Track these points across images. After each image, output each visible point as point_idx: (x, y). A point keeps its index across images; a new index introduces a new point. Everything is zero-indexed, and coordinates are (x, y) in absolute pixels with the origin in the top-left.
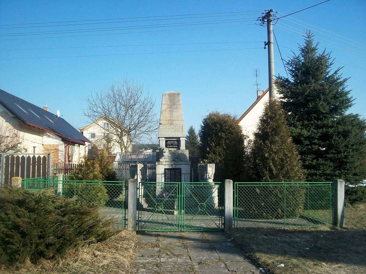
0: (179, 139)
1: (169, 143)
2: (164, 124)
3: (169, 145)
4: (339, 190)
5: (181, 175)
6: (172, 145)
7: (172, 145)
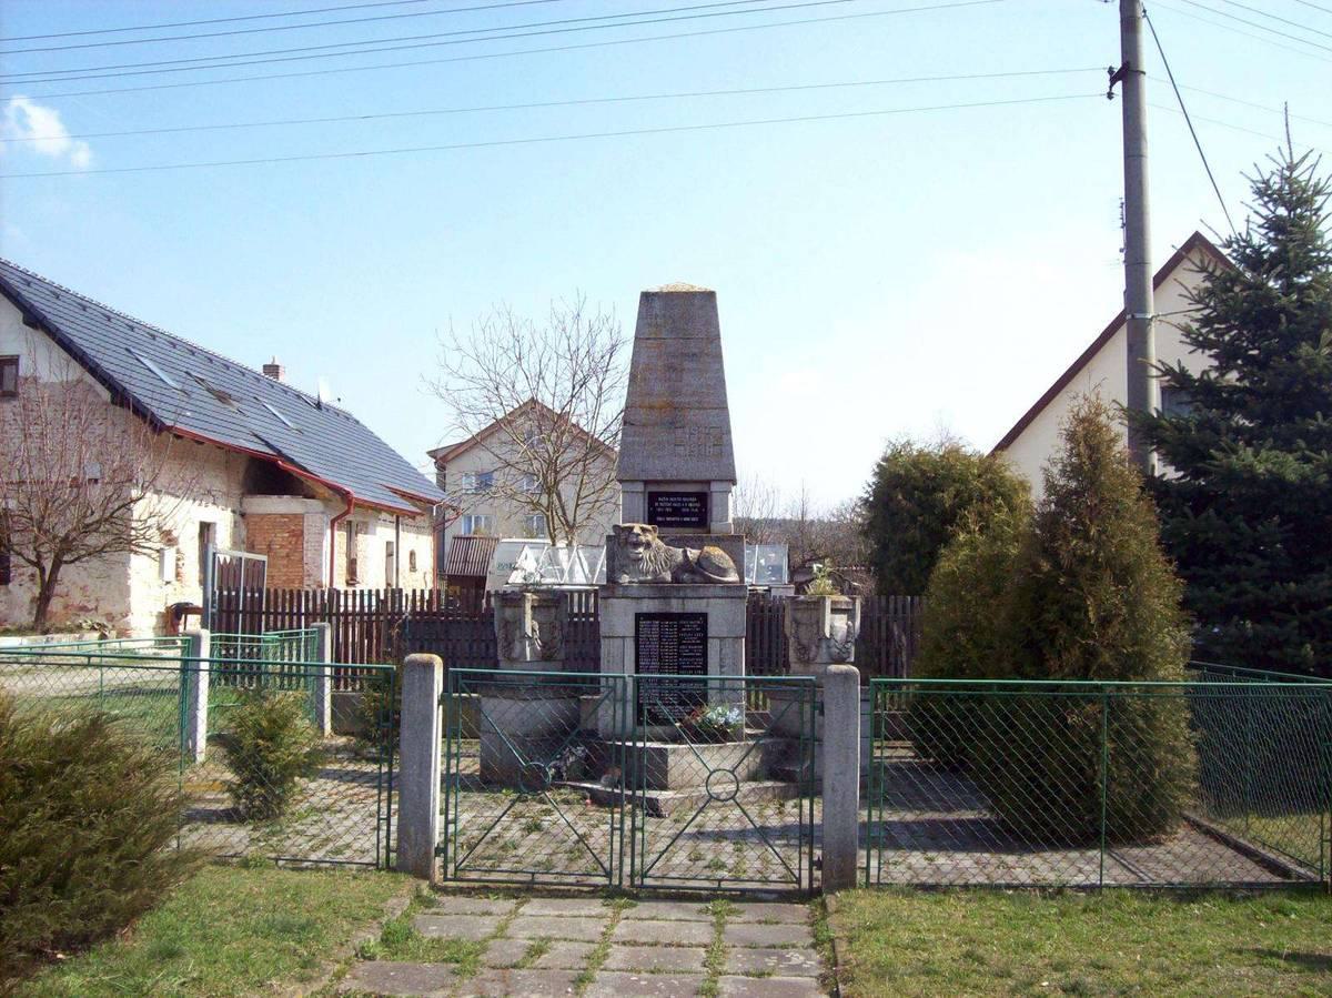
0: (705, 489)
1: (663, 502)
2: (644, 425)
3: (664, 514)
4: (193, 538)
5: (704, 640)
6: (676, 512)
7: (676, 512)
